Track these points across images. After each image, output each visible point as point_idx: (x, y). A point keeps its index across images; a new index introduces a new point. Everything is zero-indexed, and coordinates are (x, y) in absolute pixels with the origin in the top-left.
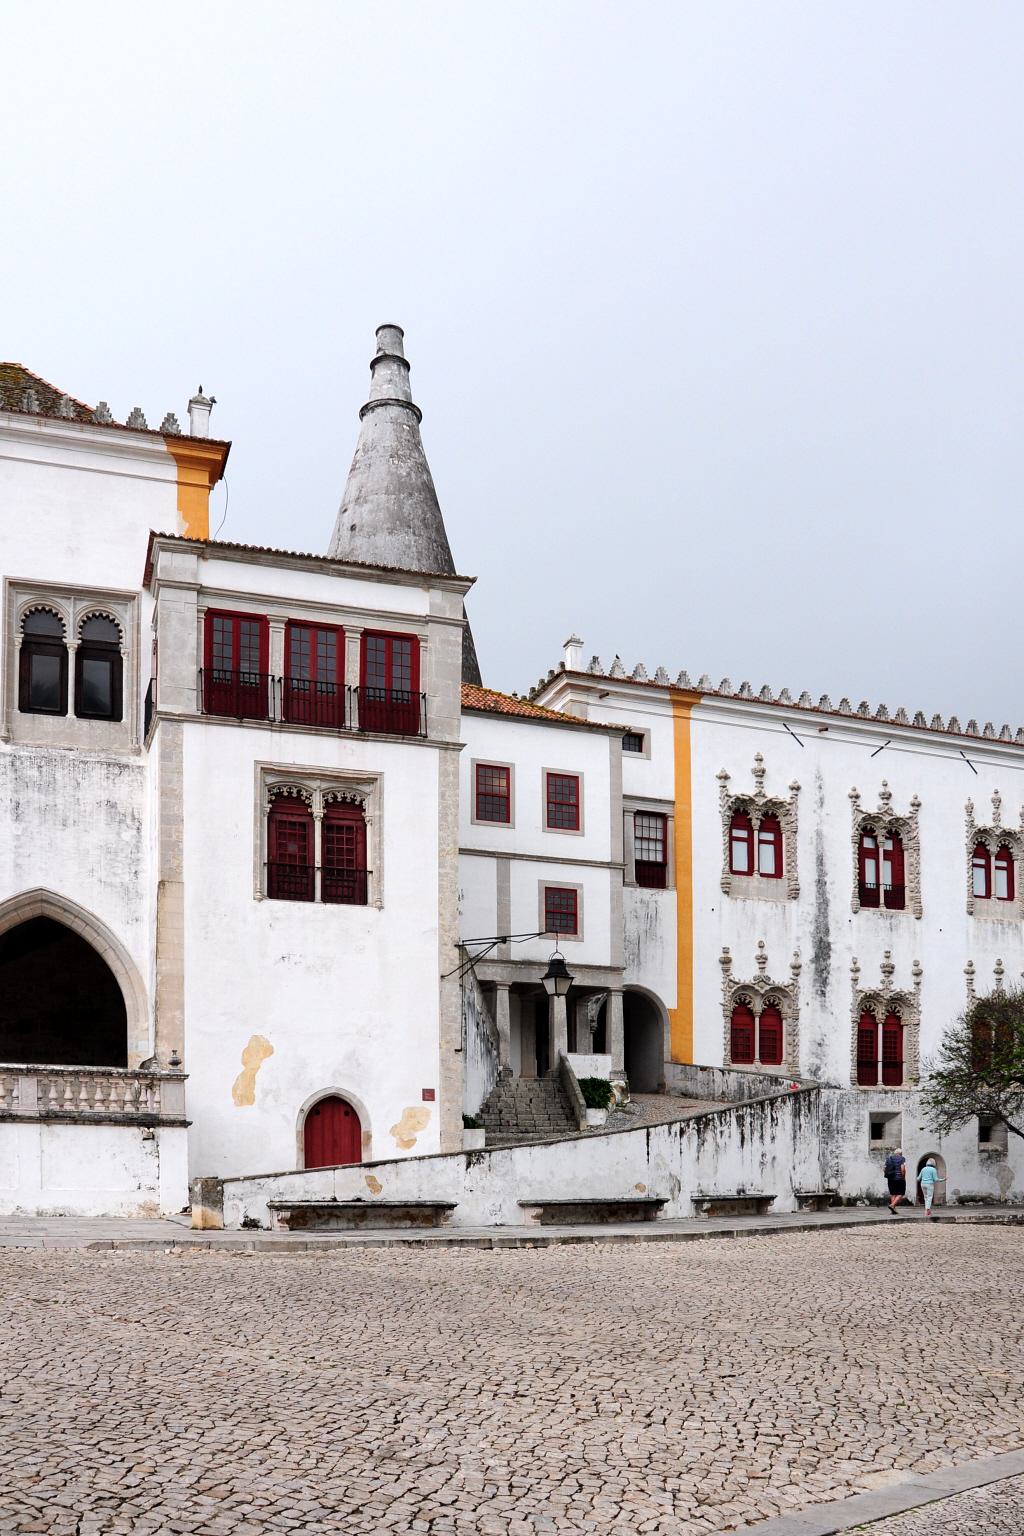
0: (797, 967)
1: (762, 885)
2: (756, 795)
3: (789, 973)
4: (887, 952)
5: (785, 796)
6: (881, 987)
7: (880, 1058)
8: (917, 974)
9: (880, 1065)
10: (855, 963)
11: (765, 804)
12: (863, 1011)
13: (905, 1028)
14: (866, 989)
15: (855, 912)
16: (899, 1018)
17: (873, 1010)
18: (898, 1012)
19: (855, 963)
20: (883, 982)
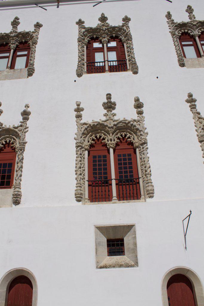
0: (26, 115)
1: (10, 73)
2: (11, 33)
3: (21, 118)
4: (107, 95)
5: (31, 29)
6: (104, 118)
7: (113, 176)
8: (139, 105)
9: (114, 183)
10: (78, 105)
11: (17, 36)
12: (93, 140)
13: (137, 150)
14: (90, 121)
15: (79, 75)
16: (131, 144)
17: (104, 139)
18: (129, 138)
19: (78, 105)
20: (105, 115)
